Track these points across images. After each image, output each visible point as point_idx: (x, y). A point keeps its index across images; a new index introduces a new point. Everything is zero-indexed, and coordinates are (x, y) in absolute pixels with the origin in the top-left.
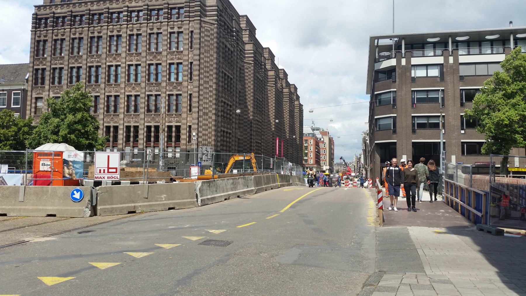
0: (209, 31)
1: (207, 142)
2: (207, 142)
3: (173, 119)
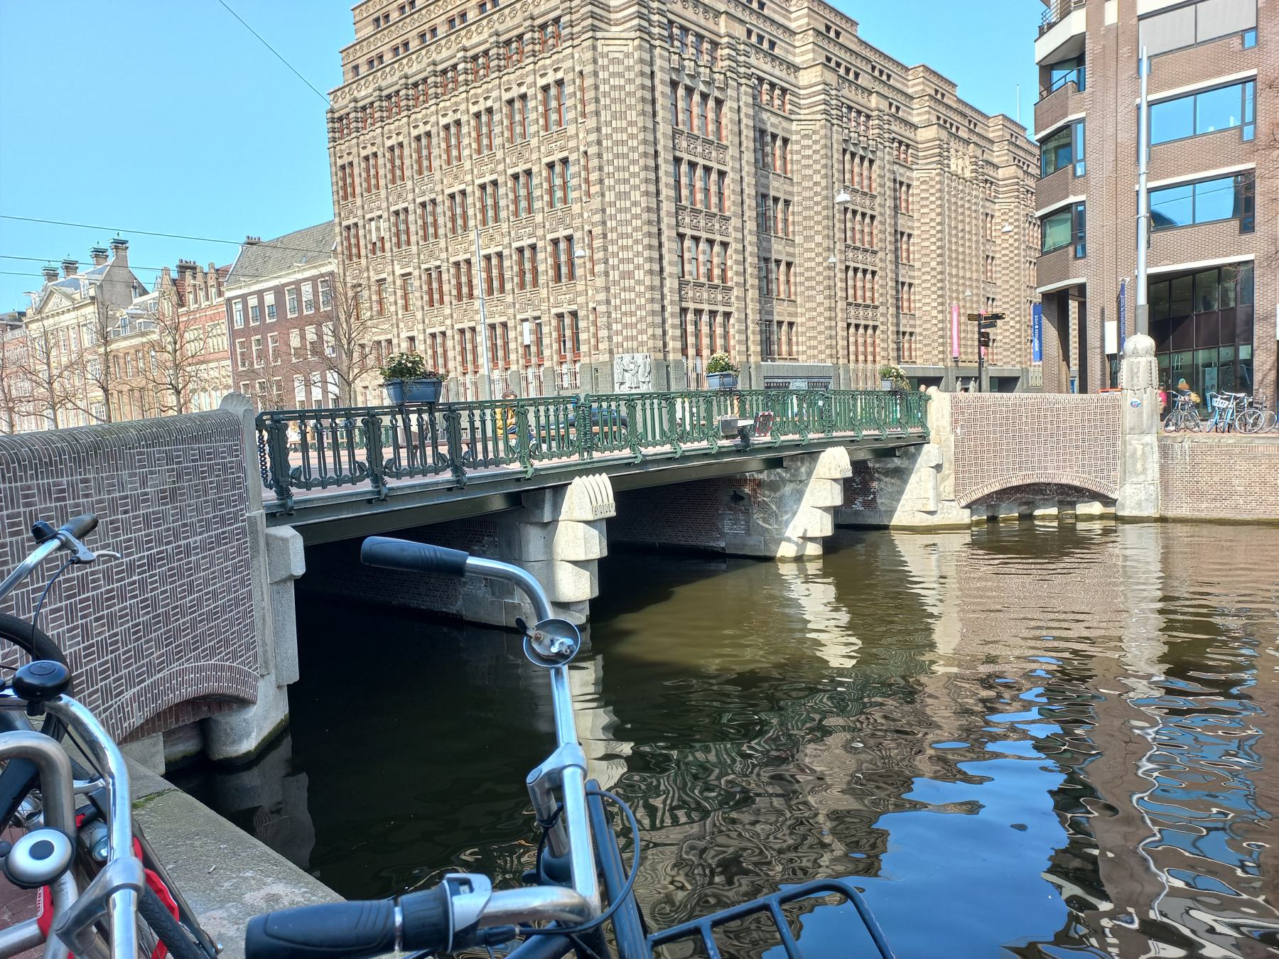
0: (620, 62)
1: (635, 343)
2: (635, 343)
3: (563, 297)
